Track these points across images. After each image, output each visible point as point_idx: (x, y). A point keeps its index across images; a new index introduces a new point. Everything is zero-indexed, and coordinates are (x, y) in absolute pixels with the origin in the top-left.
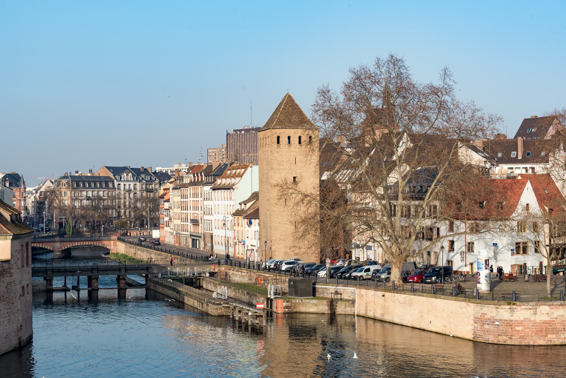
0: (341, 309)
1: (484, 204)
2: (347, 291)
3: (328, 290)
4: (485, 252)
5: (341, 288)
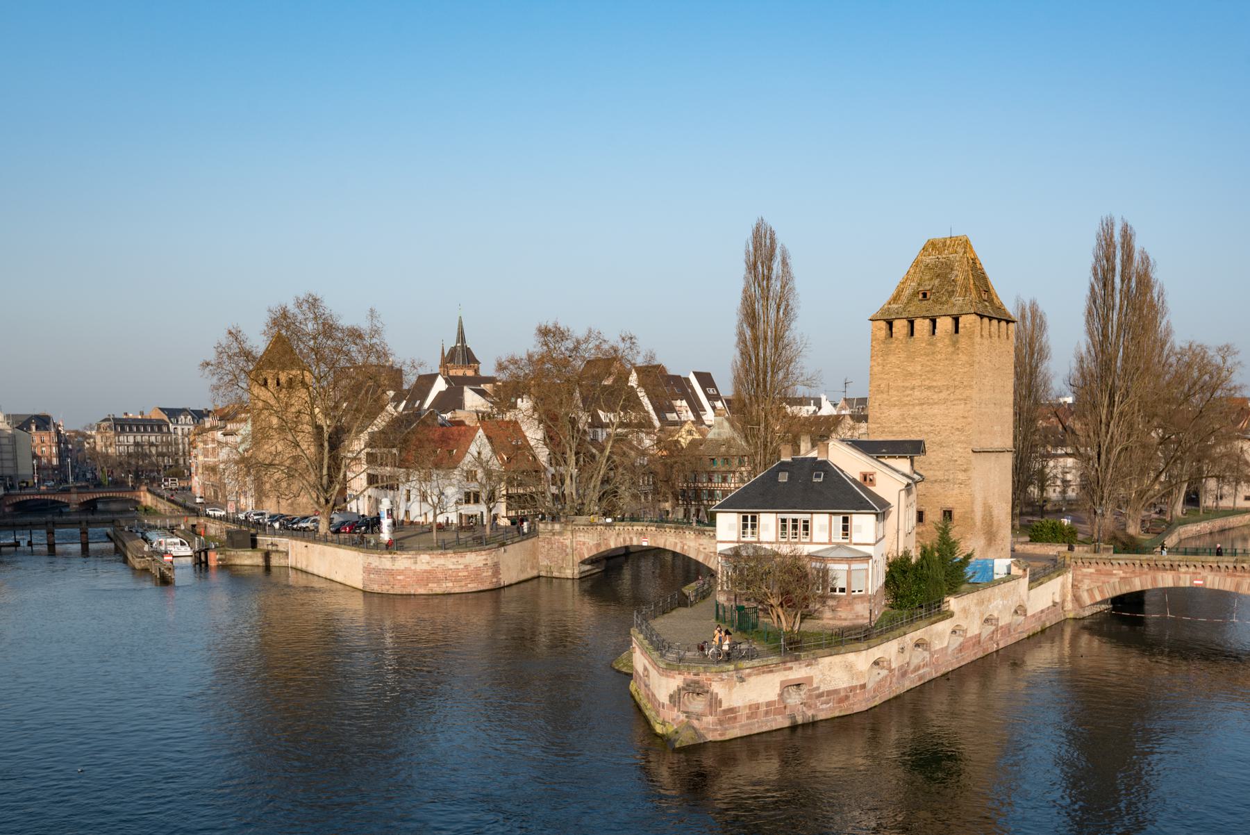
0: (275, 561)
2: (284, 543)
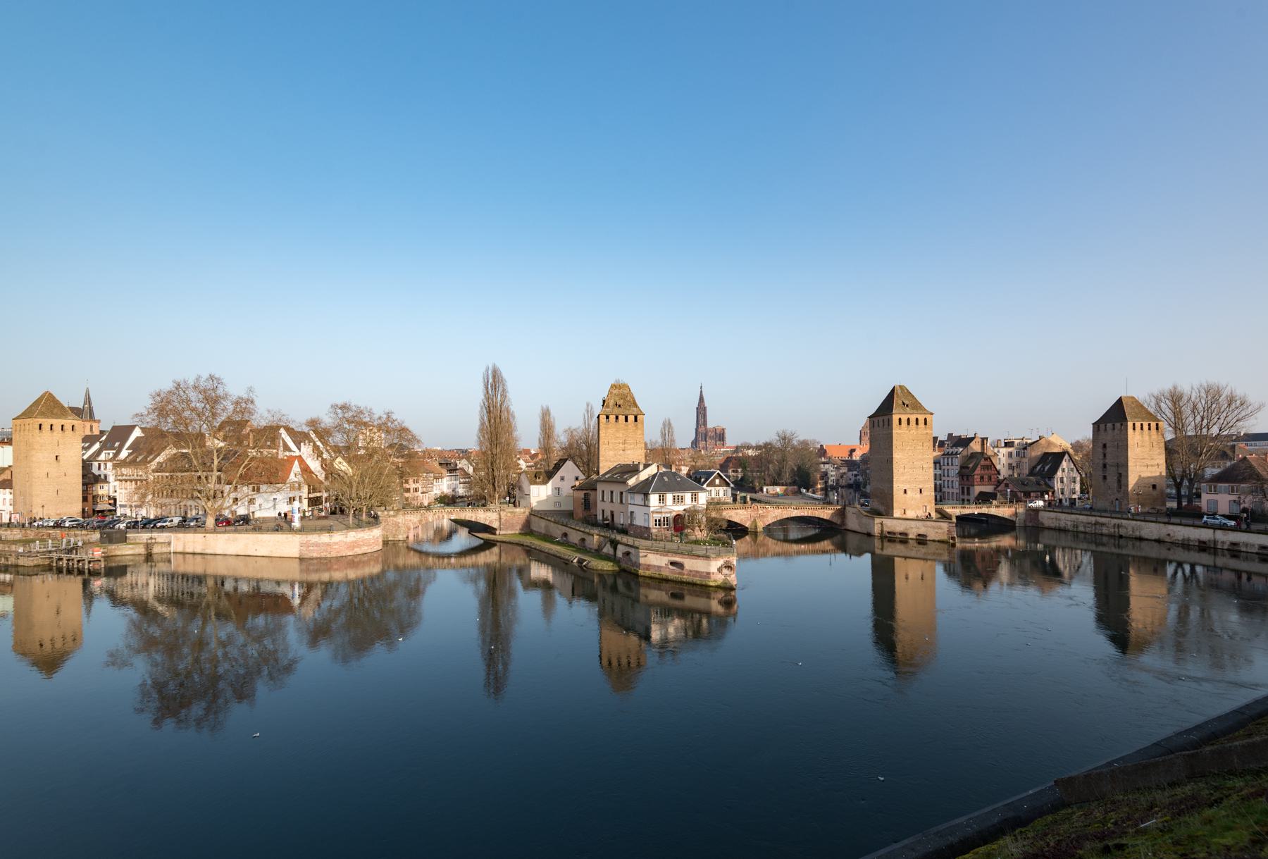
0: (156, 550)
1: (272, 474)
2: (161, 537)
3: (144, 536)
4: (267, 505)
5: (155, 535)
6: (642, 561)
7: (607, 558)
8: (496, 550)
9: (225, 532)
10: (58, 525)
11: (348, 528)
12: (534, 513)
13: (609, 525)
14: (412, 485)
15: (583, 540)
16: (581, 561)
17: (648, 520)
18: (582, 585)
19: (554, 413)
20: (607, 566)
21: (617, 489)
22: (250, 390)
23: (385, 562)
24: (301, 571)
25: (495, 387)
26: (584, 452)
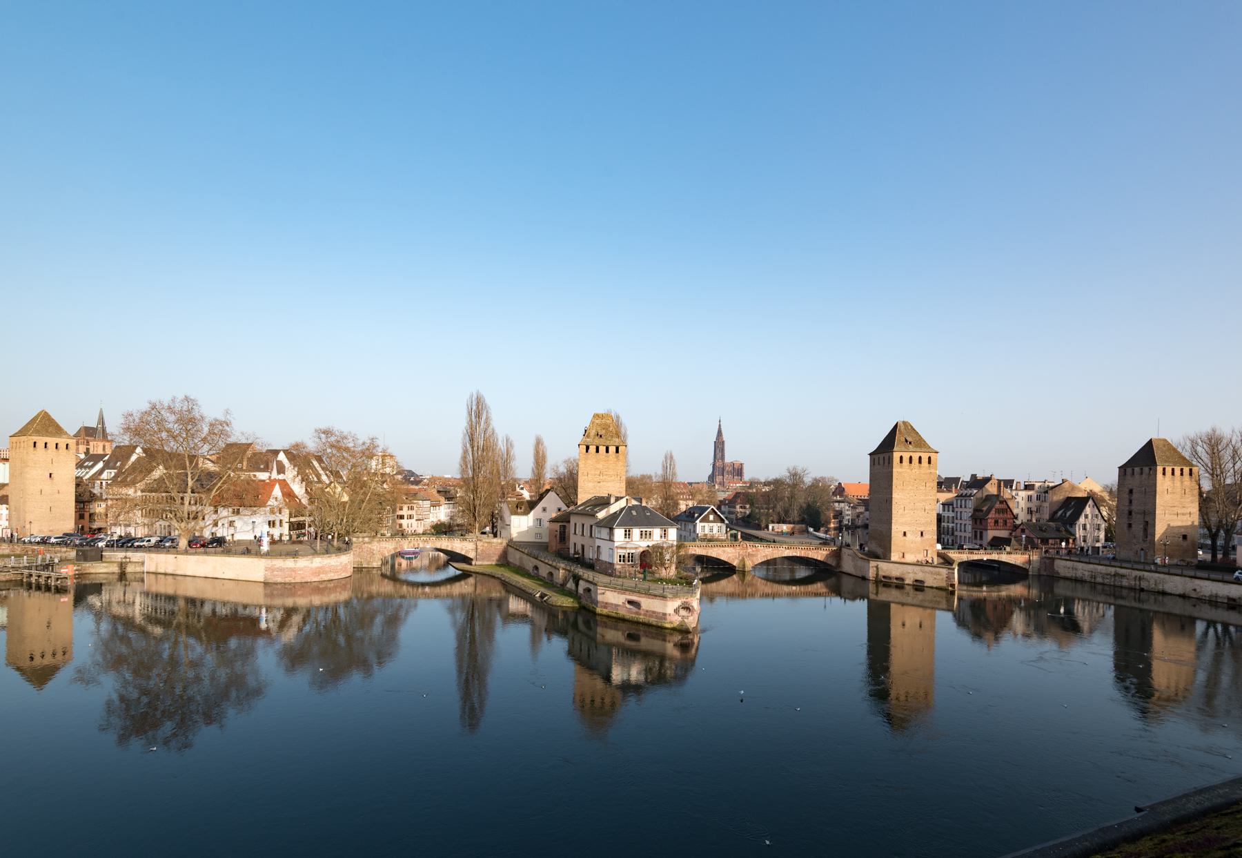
0: (130, 569)
2: (135, 556)
3: (119, 555)
4: (247, 527)
5: (129, 554)
6: (600, 598)
7: (569, 594)
8: (471, 580)
9: (196, 554)
10: (44, 541)
11: (315, 553)
12: (511, 544)
13: (581, 561)
14: (405, 512)
15: (551, 574)
16: (542, 596)
17: (612, 556)
18: (557, 623)
19: (547, 442)
20: (567, 602)
21: (588, 522)
22: (227, 412)
23: (355, 590)
24: (266, 595)
25: (478, 416)
26: (567, 485)
